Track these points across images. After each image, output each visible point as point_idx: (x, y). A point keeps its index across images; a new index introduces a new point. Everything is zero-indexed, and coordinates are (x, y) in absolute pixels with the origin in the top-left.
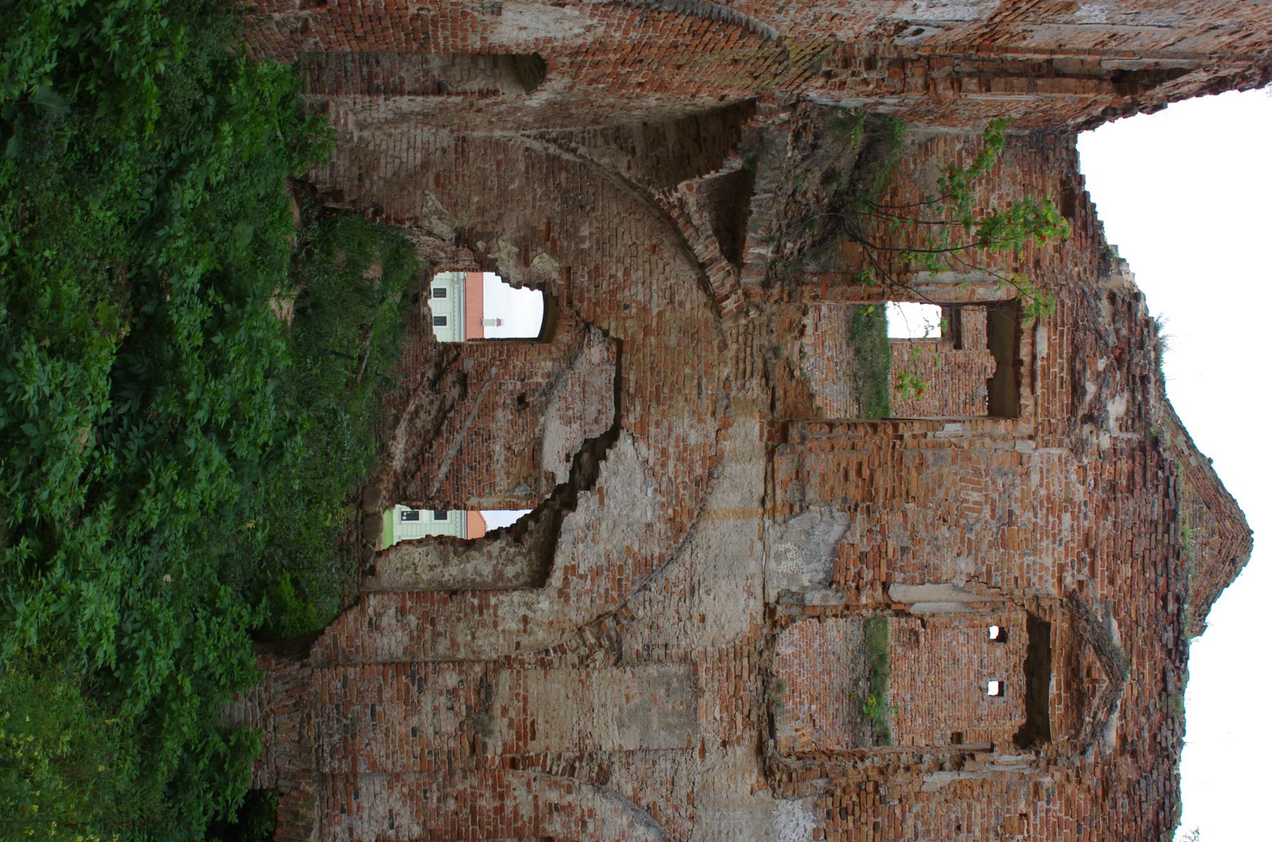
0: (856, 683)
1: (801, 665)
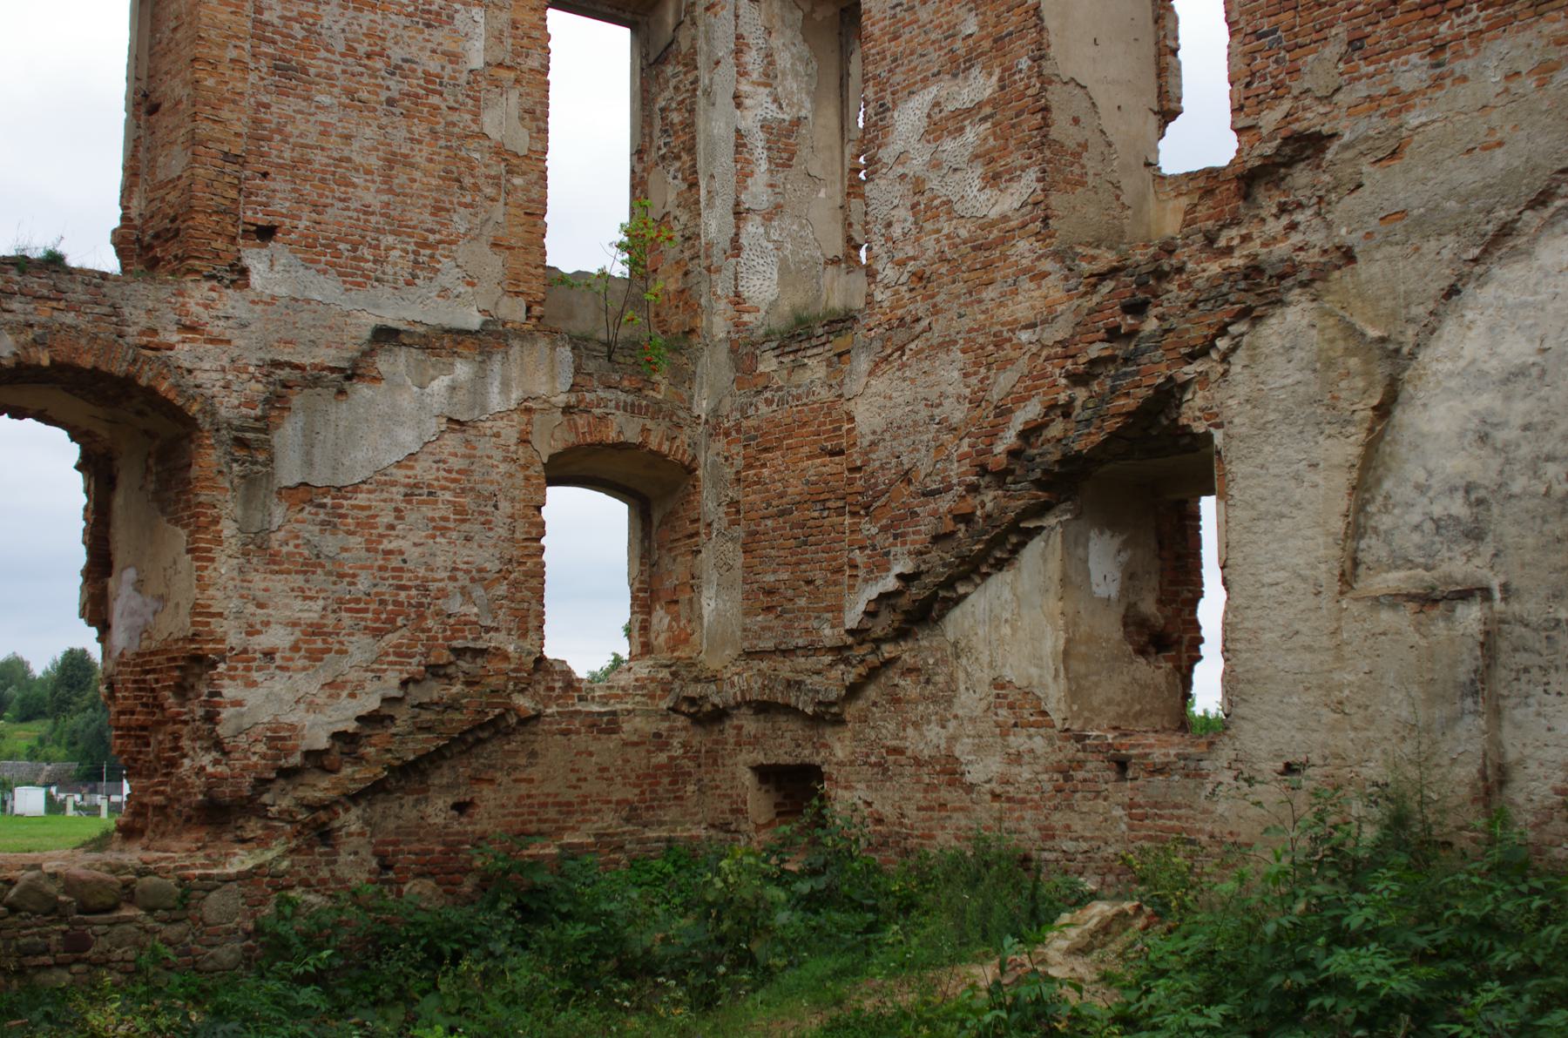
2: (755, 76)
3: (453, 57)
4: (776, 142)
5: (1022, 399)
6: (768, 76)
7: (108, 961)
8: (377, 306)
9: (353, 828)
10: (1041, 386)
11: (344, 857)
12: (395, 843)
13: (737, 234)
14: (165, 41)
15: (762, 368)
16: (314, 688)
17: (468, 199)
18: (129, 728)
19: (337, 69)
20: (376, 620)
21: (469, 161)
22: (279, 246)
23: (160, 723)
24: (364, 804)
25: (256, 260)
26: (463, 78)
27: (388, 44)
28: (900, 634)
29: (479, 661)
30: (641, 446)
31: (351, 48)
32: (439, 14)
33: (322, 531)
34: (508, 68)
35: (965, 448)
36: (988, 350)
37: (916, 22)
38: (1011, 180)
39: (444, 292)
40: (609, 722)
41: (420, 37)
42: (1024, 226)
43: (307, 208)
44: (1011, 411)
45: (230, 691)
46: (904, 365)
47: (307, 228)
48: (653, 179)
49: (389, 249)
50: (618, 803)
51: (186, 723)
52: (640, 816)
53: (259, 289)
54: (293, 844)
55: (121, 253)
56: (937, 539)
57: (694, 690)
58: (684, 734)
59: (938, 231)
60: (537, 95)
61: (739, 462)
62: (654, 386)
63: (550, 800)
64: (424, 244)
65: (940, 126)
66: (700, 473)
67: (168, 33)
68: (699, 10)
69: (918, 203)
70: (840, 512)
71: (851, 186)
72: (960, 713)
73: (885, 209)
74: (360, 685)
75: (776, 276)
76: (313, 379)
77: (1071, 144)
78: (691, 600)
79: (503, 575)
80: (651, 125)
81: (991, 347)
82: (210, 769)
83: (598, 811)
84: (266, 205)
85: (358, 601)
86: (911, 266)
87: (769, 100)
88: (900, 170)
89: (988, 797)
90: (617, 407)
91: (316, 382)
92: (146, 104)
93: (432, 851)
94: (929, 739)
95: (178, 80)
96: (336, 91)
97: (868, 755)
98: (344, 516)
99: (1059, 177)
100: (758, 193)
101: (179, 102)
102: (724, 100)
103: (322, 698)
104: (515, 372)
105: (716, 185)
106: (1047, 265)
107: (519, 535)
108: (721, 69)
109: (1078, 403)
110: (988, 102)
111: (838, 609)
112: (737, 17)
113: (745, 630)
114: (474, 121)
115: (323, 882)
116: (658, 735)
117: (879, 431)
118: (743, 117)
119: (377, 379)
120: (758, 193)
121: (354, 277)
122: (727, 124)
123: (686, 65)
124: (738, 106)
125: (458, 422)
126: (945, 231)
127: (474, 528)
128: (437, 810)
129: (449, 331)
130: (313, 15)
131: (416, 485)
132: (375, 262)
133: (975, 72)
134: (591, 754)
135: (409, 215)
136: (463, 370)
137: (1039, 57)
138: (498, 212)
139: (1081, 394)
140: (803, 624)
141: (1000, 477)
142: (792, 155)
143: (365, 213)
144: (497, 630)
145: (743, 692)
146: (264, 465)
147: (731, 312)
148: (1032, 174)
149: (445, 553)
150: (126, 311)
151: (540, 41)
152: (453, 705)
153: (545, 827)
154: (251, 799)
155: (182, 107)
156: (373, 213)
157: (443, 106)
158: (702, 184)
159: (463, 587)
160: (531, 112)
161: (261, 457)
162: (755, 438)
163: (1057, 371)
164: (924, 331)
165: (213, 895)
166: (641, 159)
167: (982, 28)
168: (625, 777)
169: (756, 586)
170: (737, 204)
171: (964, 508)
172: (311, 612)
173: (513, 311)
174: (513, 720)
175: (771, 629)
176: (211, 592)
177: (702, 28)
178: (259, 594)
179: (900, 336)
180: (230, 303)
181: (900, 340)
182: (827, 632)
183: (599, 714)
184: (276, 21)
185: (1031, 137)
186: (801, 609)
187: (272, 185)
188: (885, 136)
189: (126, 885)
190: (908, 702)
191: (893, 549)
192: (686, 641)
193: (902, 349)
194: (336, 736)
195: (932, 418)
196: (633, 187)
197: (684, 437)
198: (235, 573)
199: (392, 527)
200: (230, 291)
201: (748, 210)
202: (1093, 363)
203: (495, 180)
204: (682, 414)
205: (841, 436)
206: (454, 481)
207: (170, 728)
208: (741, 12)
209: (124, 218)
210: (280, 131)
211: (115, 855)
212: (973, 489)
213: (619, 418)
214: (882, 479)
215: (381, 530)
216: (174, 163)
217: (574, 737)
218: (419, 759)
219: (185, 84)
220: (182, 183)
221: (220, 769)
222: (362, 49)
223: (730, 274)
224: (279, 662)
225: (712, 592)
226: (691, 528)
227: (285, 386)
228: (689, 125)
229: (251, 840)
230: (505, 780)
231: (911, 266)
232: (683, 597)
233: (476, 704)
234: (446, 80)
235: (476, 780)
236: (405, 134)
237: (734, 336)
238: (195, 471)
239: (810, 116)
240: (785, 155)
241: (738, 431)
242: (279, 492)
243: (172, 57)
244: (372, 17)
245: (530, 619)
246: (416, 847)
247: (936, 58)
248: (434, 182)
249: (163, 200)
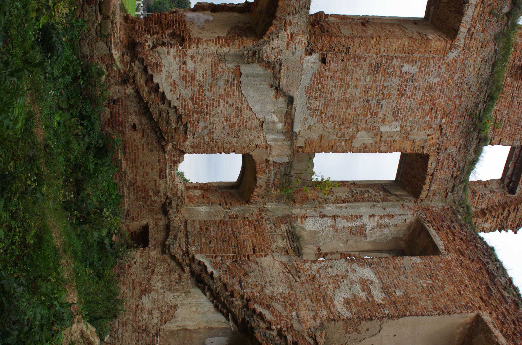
0: (477, 106)
1: (442, 91)
2: (380, 221)
3: (383, 121)
4: (358, 229)
5: (273, 313)
6: (381, 226)
7: (83, 11)
8: (300, 97)
9: (127, 91)
10: (277, 320)
11: (117, 88)
12: (122, 105)
13: (327, 216)
14: (386, 28)
15: (282, 225)
16: (174, 78)
17: (337, 127)
18: (161, 18)
19: (378, 83)
20: (196, 98)
21: (349, 127)
22: (320, 65)
23: (162, 28)
24: (135, 94)
25: (314, 58)
26: (377, 125)
27: (387, 100)
28: (193, 273)
29: (183, 132)
30: (256, 186)
31: (385, 88)
32: (397, 116)
33: (226, 80)
34: (380, 140)
35: (256, 294)
36: (290, 302)
37: (400, 275)
38: (347, 308)
39: (305, 119)
40: (163, 176)
41: (389, 110)
42: (332, 313)
43: (332, 74)
44: (269, 309)
45: (173, 50)
46: (284, 273)
47: (326, 74)
48: (345, 188)
49: (319, 101)
50: (136, 179)
51: (162, 36)
52: (131, 186)
53: (305, 59)
54: (122, 71)
55: (316, 14)
56: (225, 285)
57: (174, 204)
58: (159, 201)
59: (329, 284)
60: (372, 149)
61: (251, 218)
62: (276, 190)
63: (137, 156)
64: (321, 113)
65: (365, 284)
66: (247, 205)
67: (388, 29)
68: (402, 202)
69: (339, 277)
70: (234, 252)
71: (344, 254)
72: (166, 294)
73: (336, 266)
74: (175, 93)
75: (313, 230)
76: (276, 77)
77: (360, 328)
78: (204, 203)
79: (212, 140)
80: (363, 187)
81: (290, 302)
82: (147, 44)
83: (133, 172)
84: (333, 61)
85: (203, 92)
87: (373, 227)
88: (350, 271)
89: (137, 304)
90: (268, 177)
91: (275, 78)
92: (365, 22)
93: (119, 117)
94: (157, 283)
95: (373, 32)
96: (371, 83)
97: (151, 263)
98: (231, 87)
99: (348, 324)
100: (341, 223)
101: (366, 32)
102: (372, 211)
103: (170, 80)
104: (279, 143)
105: (344, 209)
106: (318, 321)
107: (225, 145)
108: (383, 210)
109: (272, 332)
110: (373, 300)
111: (201, 252)
112: (400, 215)
113: (194, 221)
114: (362, 128)
115: (109, 81)
116: (159, 192)
117: (262, 265)
118: (366, 218)
119: (276, 97)
120: (341, 223)
121: (310, 90)
122: (364, 213)
123: (383, 198)
124: (370, 216)
125: (263, 124)
126: (329, 286)
127: (227, 130)
128: (133, 119)
129: (293, 121)
130: (395, 75)
131: (241, 111)
132: (315, 96)
133: (383, 295)
134: (152, 170)
135: (331, 107)
136: (280, 126)
137: (389, 317)
138: (333, 137)
139: (275, 333)
140: (196, 240)
141: (246, 306)
142: (354, 235)
143: (331, 93)
144: (193, 138)
145: (173, 220)
146: (247, 61)
147: (301, 215)
148: (349, 315)
149: (219, 121)
150: (297, 16)
151: (390, 150)
152: (168, 124)
153: (128, 155)
154: (137, 57)
155: (364, 33)
156: (331, 96)
157: (367, 118)
158: (344, 205)
159: (207, 127)
160: (366, 147)
161: (250, 60)
162: (259, 223)
163: (282, 325)
164: (295, 280)
165: (105, 45)
166: (352, 184)
167: (398, 297)
168: (144, 181)
169: (209, 224)
170: (337, 216)
171: (236, 294)
172: (199, 77)
173: (300, 142)
174: (163, 143)
175: (194, 229)
176: (205, 44)
177: (396, 203)
178: (205, 60)
179: (294, 272)
180: (300, 49)
181: (292, 271)
182: (194, 249)
183: (166, 173)
184: (393, 63)
185: (362, 314)
186: (201, 240)
187: (339, 63)
188: (361, 265)
189: (108, 17)
190: (170, 276)
191: (221, 270)
192: (190, 201)
193: (289, 272)
194: (158, 85)
195: (266, 283)
196: (342, 182)
197: (259, 200)
198: (211, 52)
199: (227, 103)
200: (304, 49)
201: (335, 220)
202: (285, 337)
203: (343, 136)
204: (267, 199)
205: (259, 252)
206: (243, 123)
207: (160, 31)
208: (402, 216)
209: (328, 15)
210: (357, 65)
211: (119, 14)
212: (242, 297)
213: (265, 178)
214: (245, 266)
215: (226, 99)
216: (346, 31)
217: (158, 164)
218: (150, 113)
219: (371, 34)
220: (339, 34)
221: (147, 47)
222: (385, 91)
223: (314, 214)
224: (182, 66)
225: (207, 210)
226: (228, 202)
227: (273, 67)
228: (363, 200)
229: (123, 57)
230: (143, 141)
231: (317, 275)
232: (205, 200)
233: (168, 131)
234: (376, 119)
235: (143, 132)
236: (357, 106)
237: (293, 216)
238: (245, 38)
239: (367, 240)
240: (354, 232)
241: (261, 218)
242: (238, 66)
243: (380, 30)
244: (396, 94)
245: (197, 149)
246: (121, 112)
247: (388, 282)
248: (342, 116)
249: (334, 27)
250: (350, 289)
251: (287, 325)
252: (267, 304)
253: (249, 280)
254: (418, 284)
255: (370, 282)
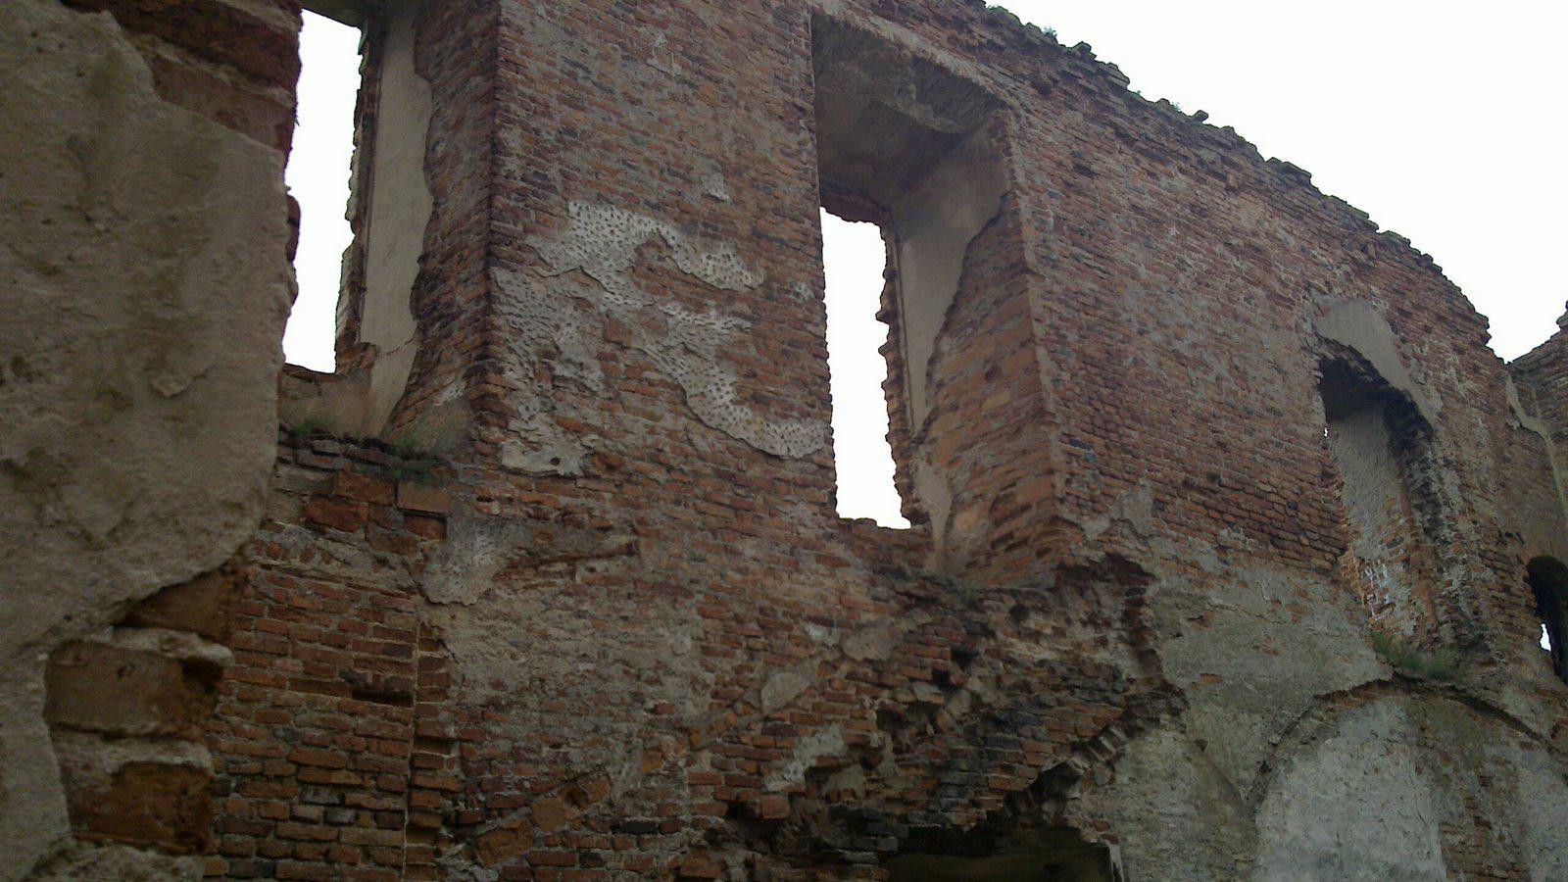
5: (814, 720)
10: (842, 712)
35: (705, 762)
44: (791, 732)
59: (653, 417)
81: (754, 627)
86: (590, 439)
117: (512, 685)
126: (668, 421)
195: (638, 697)
205: (407, 668)
212: (715, 839)
231: (590, 439)
250: (687, 351)
251: (865, 679)
252: (765, 732)
253: (625, 774)
254: (673, 87)
255: (653, 251)
